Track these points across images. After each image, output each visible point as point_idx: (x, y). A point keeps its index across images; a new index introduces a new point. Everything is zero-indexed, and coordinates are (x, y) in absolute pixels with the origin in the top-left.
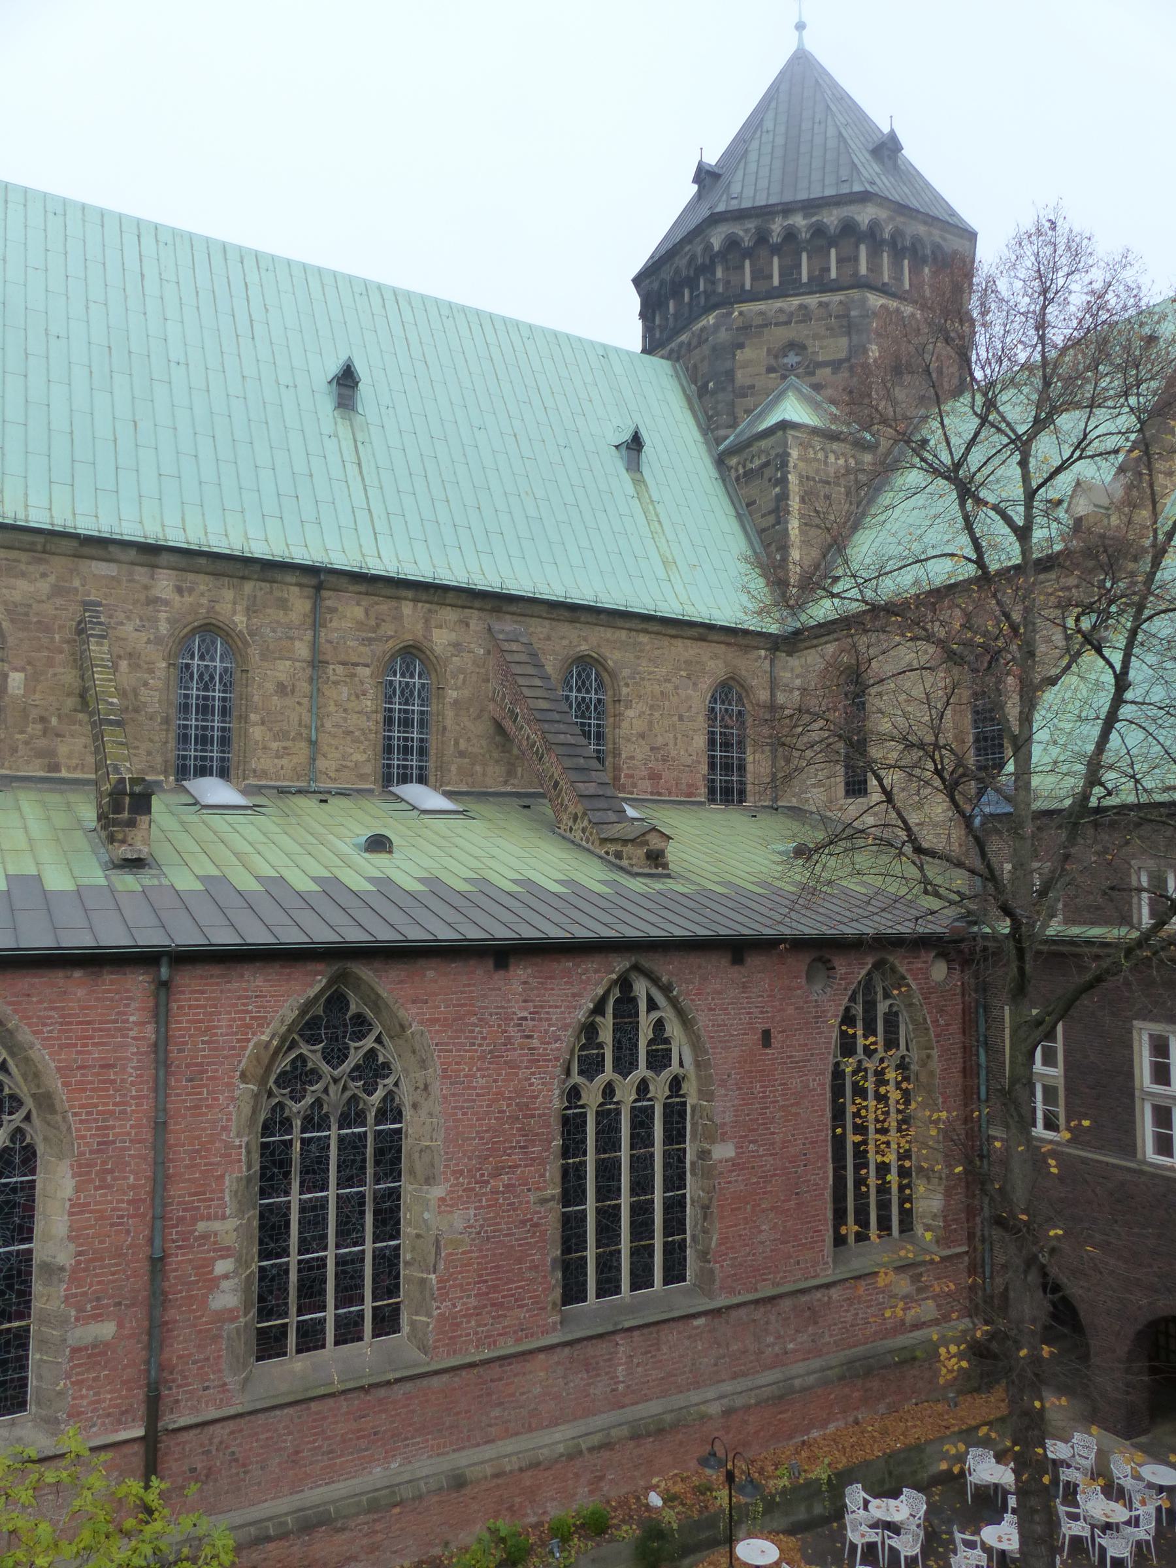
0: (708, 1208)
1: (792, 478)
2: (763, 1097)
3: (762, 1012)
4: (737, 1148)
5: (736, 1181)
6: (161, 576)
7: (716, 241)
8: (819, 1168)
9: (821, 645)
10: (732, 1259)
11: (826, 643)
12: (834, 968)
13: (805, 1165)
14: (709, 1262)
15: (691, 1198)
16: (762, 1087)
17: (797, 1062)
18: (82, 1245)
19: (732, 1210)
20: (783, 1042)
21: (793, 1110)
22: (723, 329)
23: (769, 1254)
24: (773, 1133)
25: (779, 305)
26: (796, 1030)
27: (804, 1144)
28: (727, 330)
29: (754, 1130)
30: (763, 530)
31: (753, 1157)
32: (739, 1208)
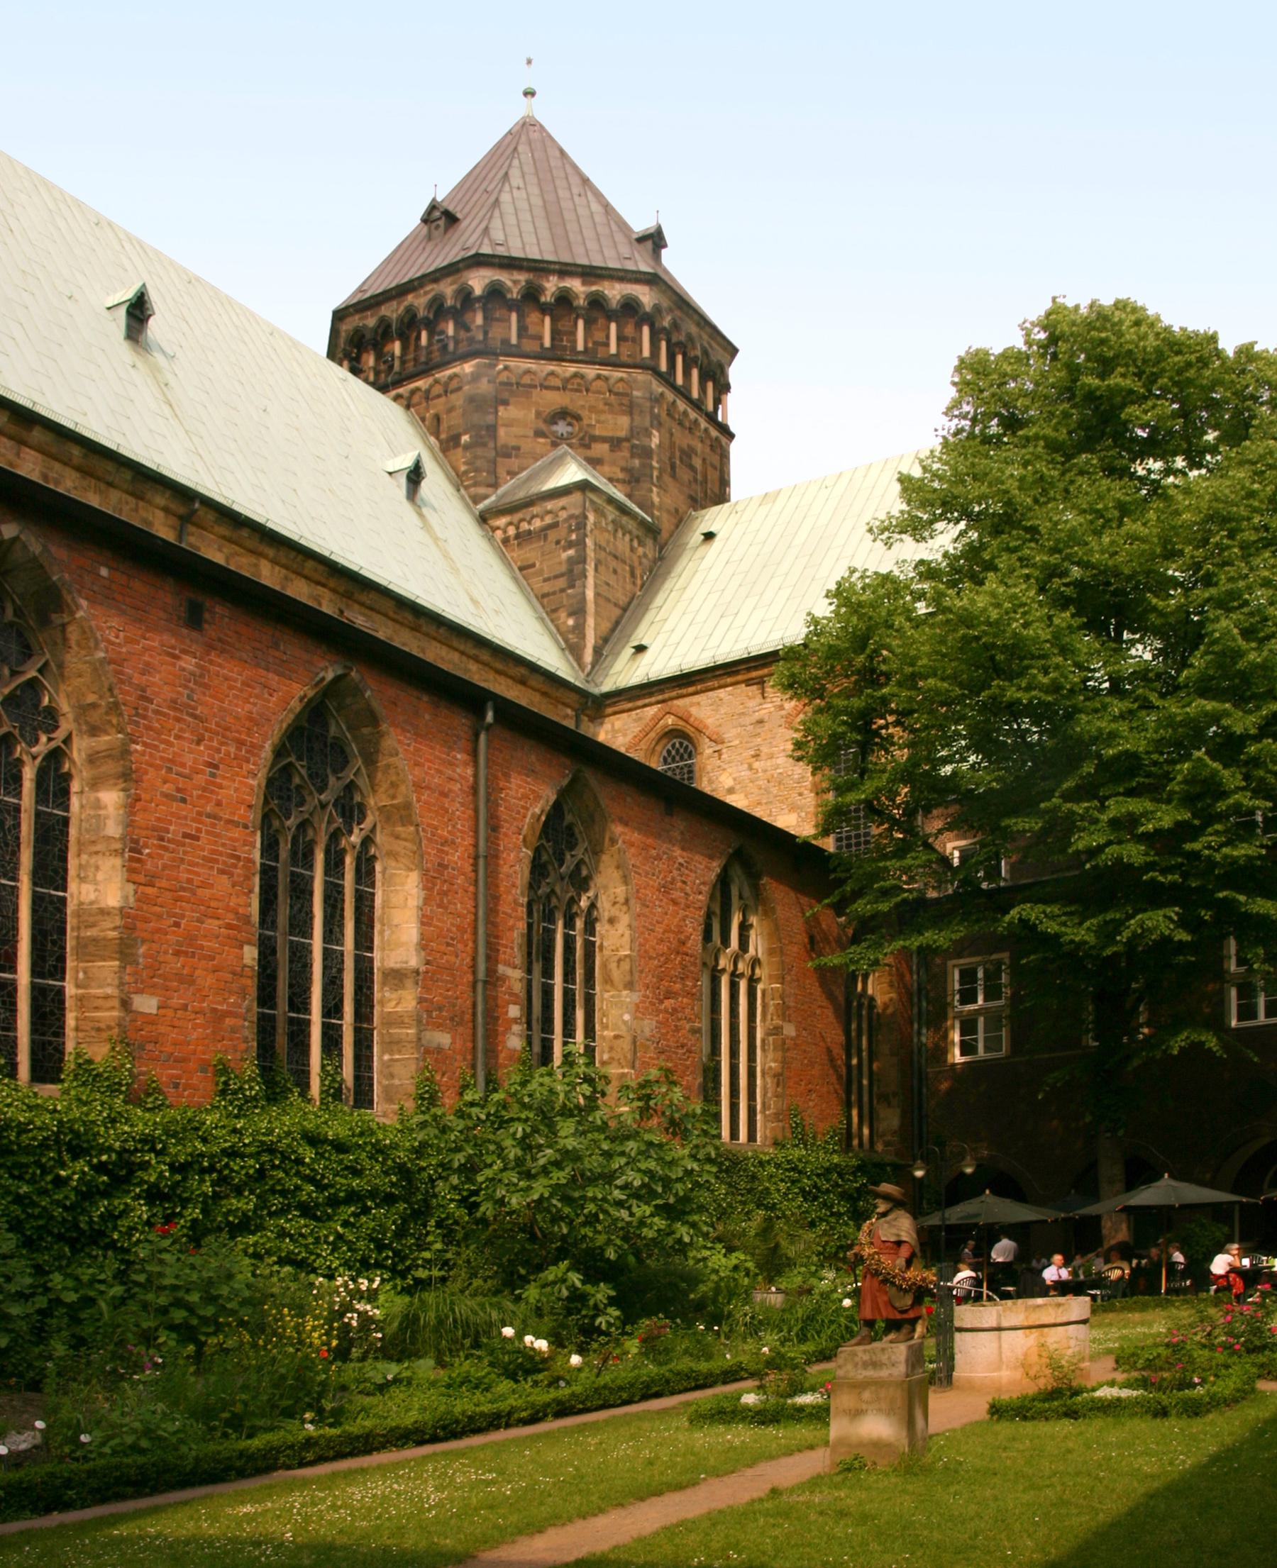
1: (589, 542)
6: (27, 457)
7: (478, 281)
18: (429, 955)
22: (485, 380)
25: (552, 368)
28: (489, 382)
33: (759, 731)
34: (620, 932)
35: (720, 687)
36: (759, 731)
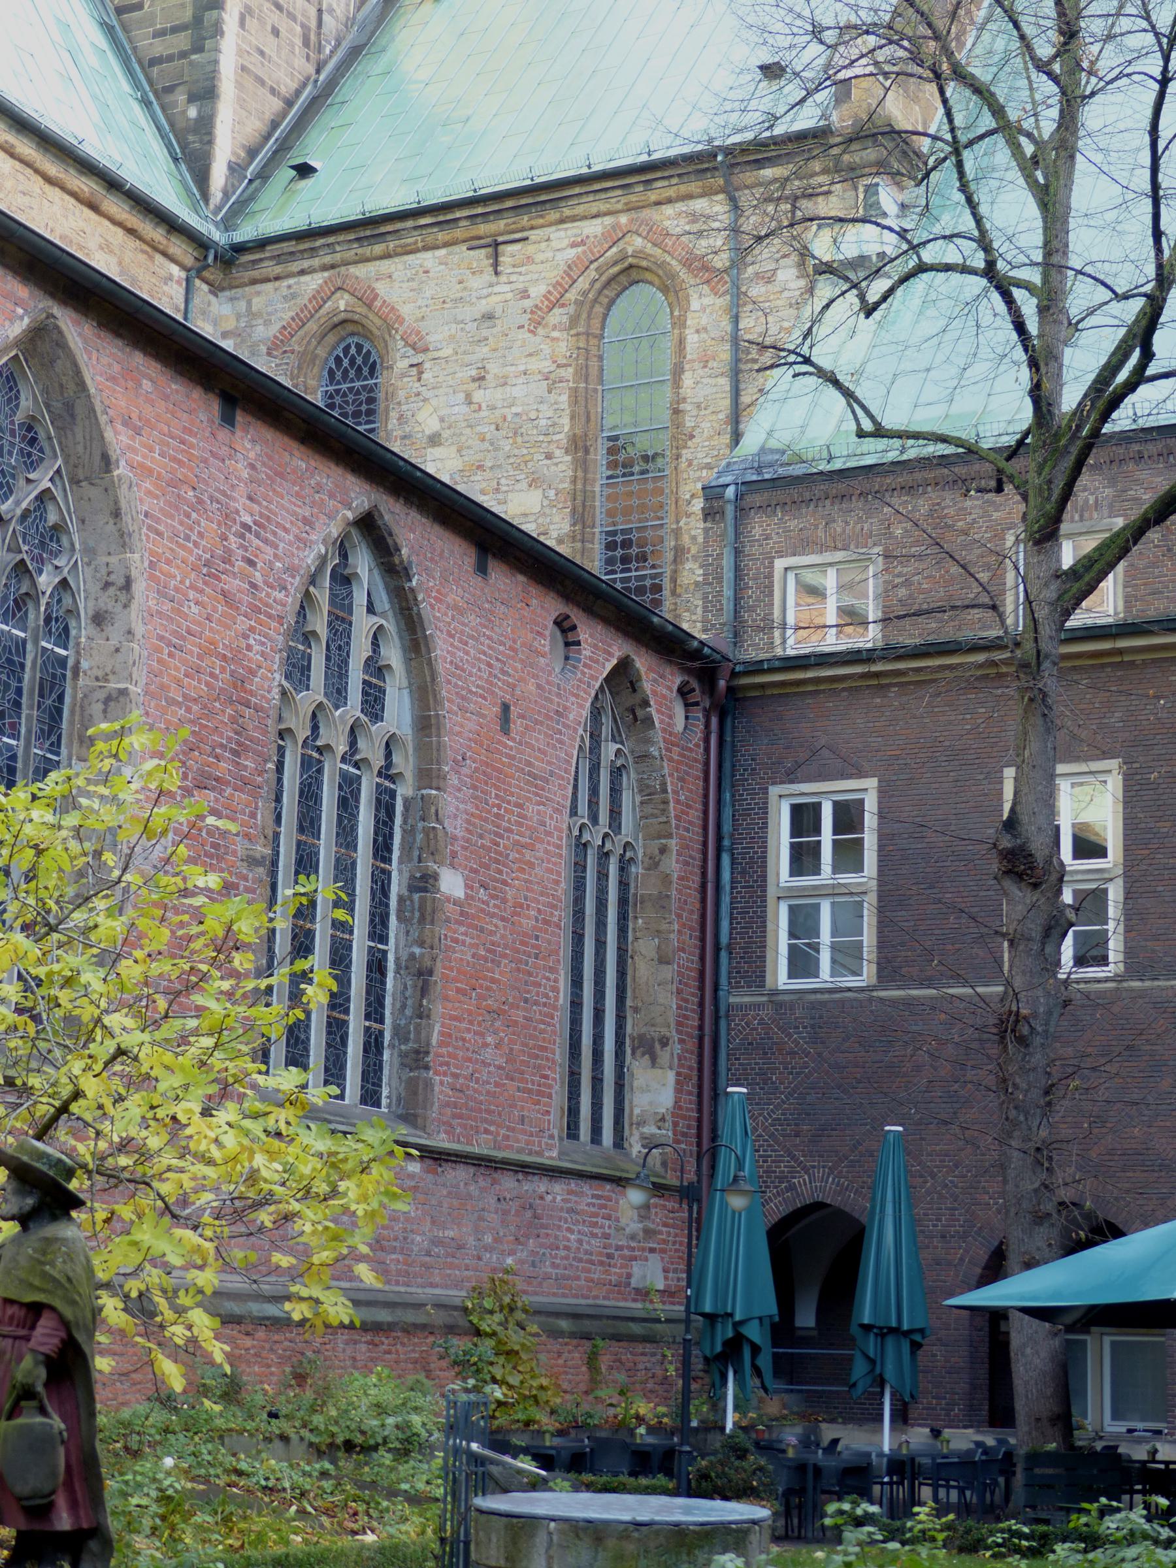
0: (430, 972)
3: (504, 673)
4: (467, 886)
9: (290, 275)
11: (302, 272)
12: (578, 643)
14: (427, 1068)
15: (397, 959)
17: (535, 777)
24: (505, 883)
30: (153, 62)
31: (483, 910)
33: (485, 333)
34: (114, 642)
35: (426, 248)
36: (485, 333)
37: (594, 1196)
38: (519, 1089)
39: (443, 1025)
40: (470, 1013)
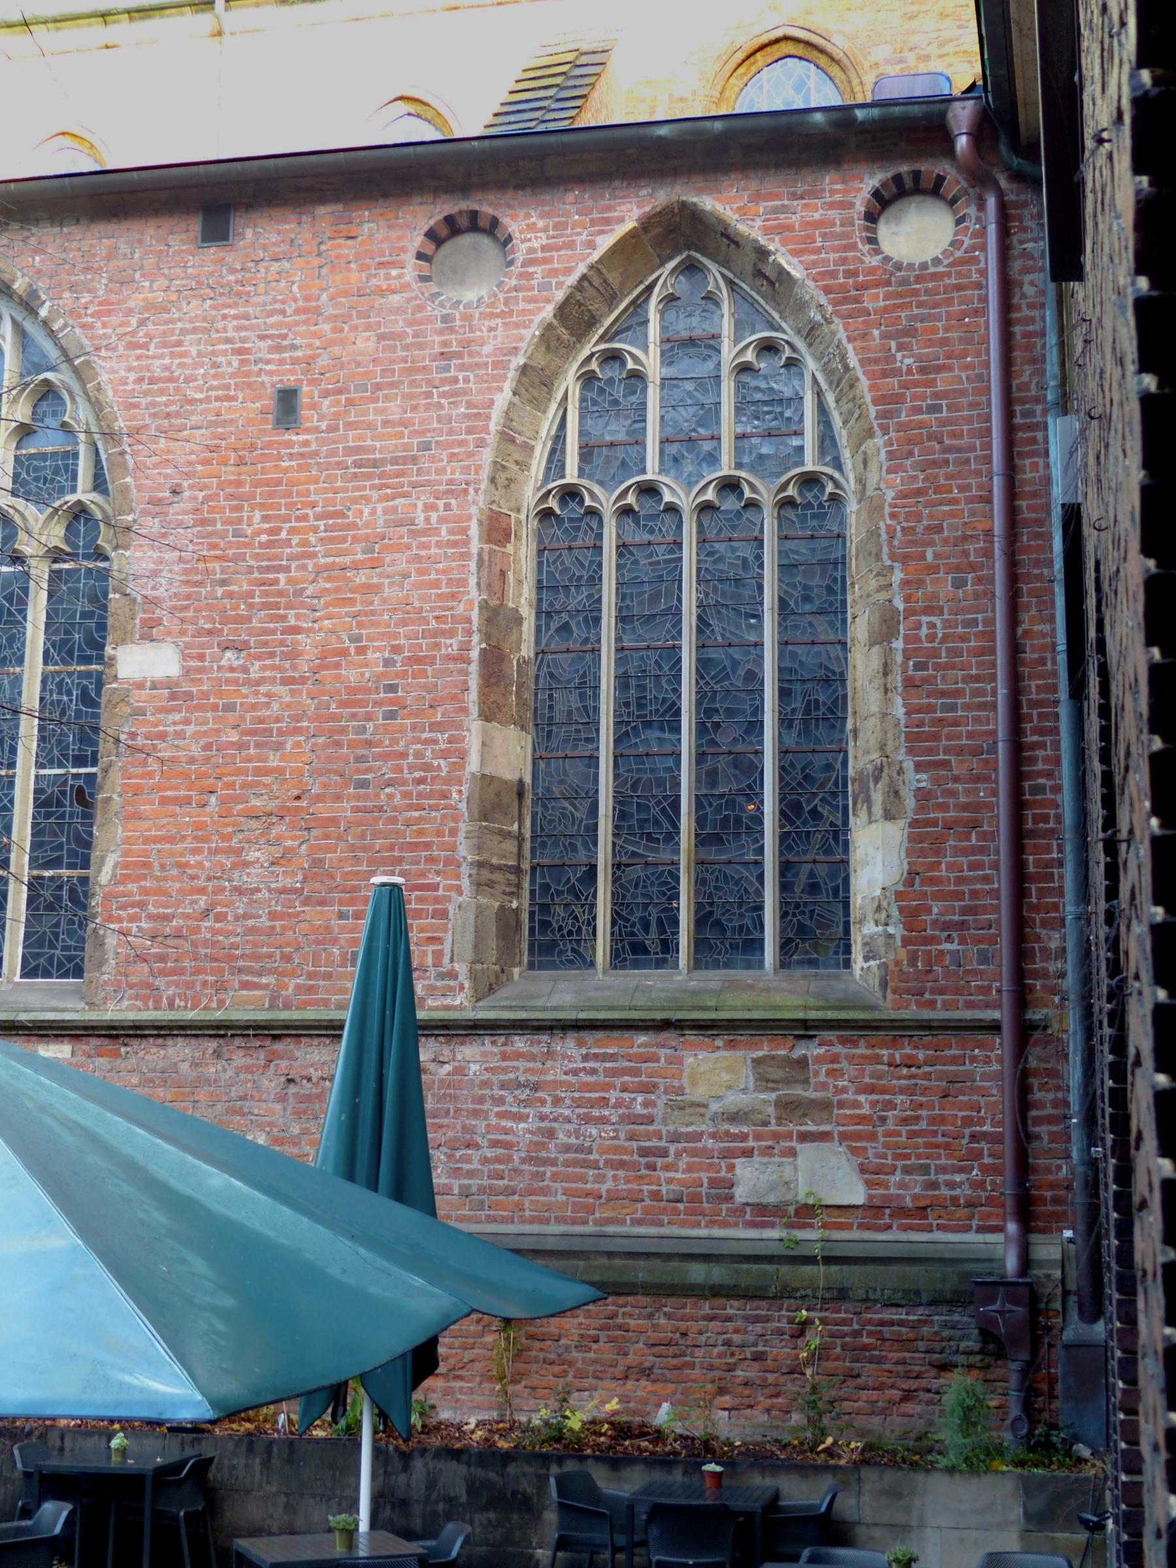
2: (269, 544)
3: (279, 349)
4: (185, 657)
5: (180, 735)
8: (435, 727)
10: (152, 917)
13: (391, 715)
16: (265, 518)
17: (375, 464)
19: (164, 801)
20: (337, 415)
21: (361, 578)
23: (264, 922)
24: (296, 630)
26: (378, 387)
27: (388, 663)
29: (239, 619)
31: (236, 682)
32: (187, 801)
37: (585, 1058)
38: (342, 916)
39: (125, 854)
40: (199, 826)
